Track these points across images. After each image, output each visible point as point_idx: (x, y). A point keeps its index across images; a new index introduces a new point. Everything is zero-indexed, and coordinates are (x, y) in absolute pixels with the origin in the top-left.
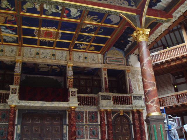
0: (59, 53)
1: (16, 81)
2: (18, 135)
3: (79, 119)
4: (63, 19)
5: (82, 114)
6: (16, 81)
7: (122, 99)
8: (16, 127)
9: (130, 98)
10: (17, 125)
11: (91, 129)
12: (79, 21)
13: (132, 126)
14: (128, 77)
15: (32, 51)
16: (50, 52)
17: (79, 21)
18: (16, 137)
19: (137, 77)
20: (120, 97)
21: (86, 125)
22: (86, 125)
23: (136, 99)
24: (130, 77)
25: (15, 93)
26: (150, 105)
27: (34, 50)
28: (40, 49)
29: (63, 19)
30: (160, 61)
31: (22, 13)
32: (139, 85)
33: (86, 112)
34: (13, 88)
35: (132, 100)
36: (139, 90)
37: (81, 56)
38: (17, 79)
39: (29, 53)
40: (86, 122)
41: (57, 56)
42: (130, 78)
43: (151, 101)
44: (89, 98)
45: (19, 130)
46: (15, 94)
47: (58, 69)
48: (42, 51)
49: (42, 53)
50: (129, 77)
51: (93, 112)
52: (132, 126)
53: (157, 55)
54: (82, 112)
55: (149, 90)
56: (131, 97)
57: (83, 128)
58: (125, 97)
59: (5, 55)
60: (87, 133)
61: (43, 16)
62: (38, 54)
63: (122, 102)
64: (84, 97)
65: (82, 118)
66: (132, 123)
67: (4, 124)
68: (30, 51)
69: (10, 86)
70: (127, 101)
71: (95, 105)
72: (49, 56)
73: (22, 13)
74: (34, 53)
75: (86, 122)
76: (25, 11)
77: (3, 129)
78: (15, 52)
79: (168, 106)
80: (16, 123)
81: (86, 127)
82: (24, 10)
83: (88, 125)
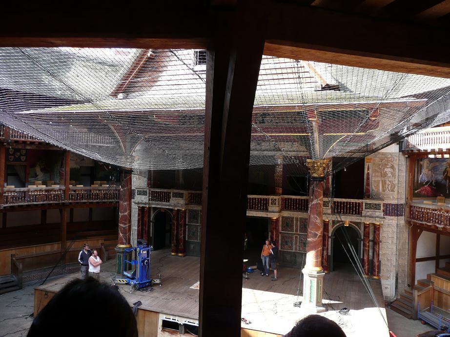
3: (287, 226)
5: (292, 221)
7: (347, 205)
11: (302, 240)
13: (362, 242)
14: (367, 169)
19: (384, 169)
20: (344, 202)
21: (296, 234)
22: (296, 234)
23: (370, 208)
24: (370, 170)
32: (385, 183)
33: (297, 219)
40: (297, 231)
42: (370, 171)
44: (303, 201)
50: (368, 169)
51: (304, 219)
52: (362, 242)
54: (292, 218)
57: (292, 238)
58: (353, 203)
60: (297, 243)
63: (347, 210)
64: (296, 199)
65: (292, 226)
66: (362, 238)
70: (356, 208)
75: (297, 231)
81: (296, 237)
83: (298, 234)
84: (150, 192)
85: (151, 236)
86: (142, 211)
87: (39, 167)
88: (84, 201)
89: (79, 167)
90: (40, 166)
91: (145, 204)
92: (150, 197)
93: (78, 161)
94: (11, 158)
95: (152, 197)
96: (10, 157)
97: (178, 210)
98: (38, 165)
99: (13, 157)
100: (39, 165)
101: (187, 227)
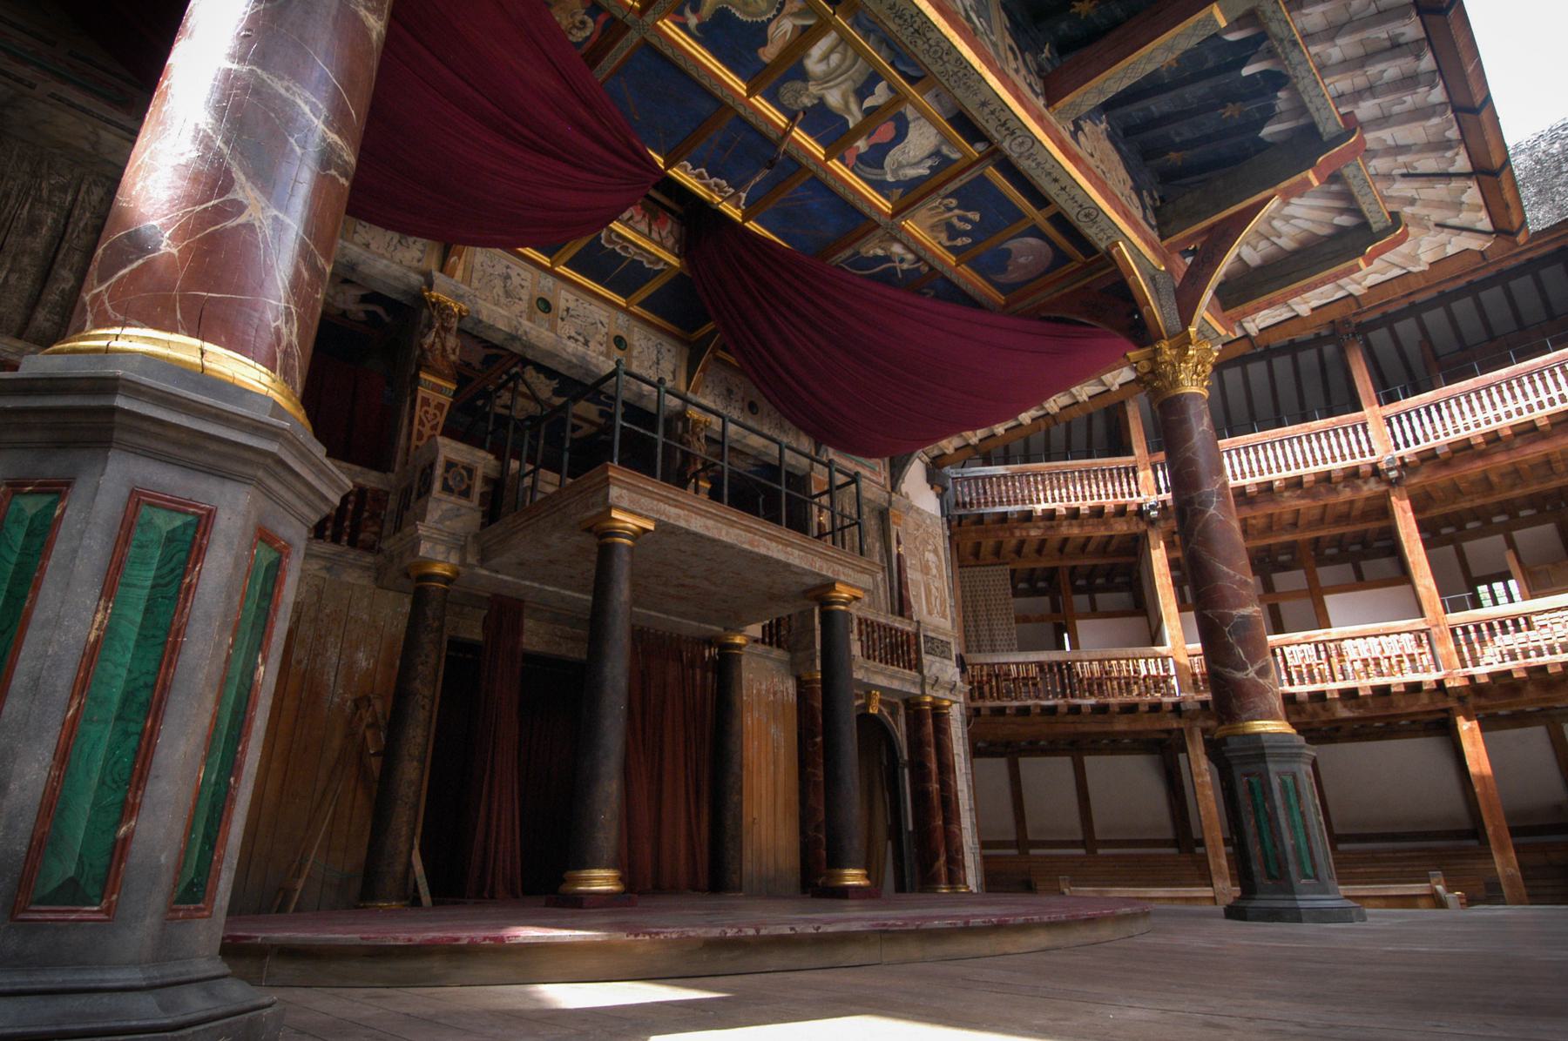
0: (643, 343)
1: (428, 426)
4: (835, 165)
6: (428, 426)
9: (913, 642)
12: (885, 206)
15: (516, 280)
16: (605, 321)
17: (885, 206)
25: (466, 494)
26: (1257, 685)
27: (524, 274)
28: (560, 284)
29: (835, 165)
30: (1018, 508)
31: (668, 27)
34: (453, 456)
35: (918, 651)
36: (930, 613)
37: (735, 390)
38: (431, 410)
39: (498, 283)
41: (635, 353)
43: (1256, 667)
46: (463, 502)
47: (586, 426)
48: (564, 299)
49: (568, 310)
50: (899, 543)
53: (1005, 476)
55: (1243, 617)
56: (917, 636)
58: (897, 630)
61: (759, 102)
62: (545, 305)
68: (508, 277)
71: (779, 646)
72: (599, 337)
73: (668, 27)
74: (525, 295)
76: (693, 21)
79: (1036, 706)
82: (695, 10)
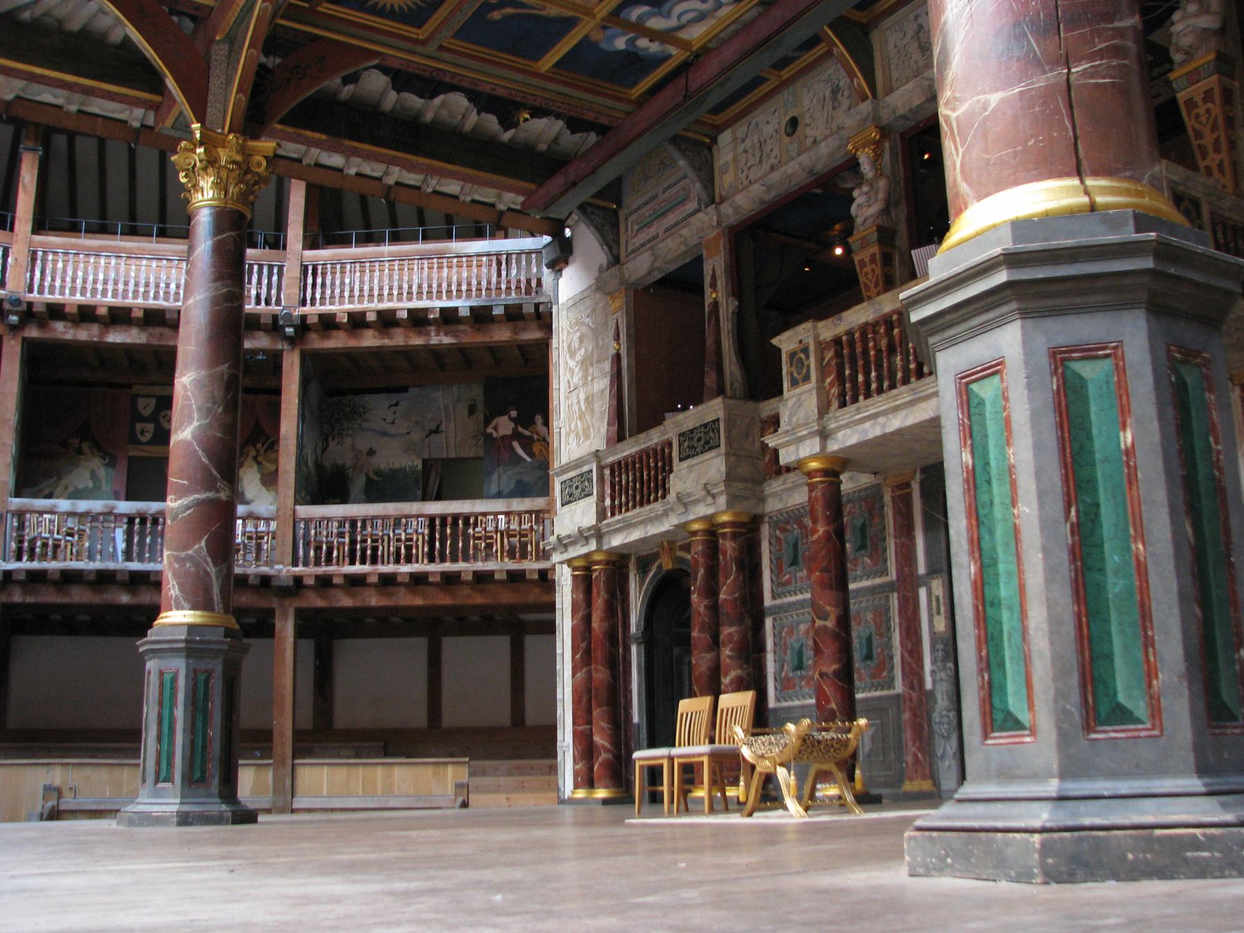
2: (940, 646)
6: (872, 285)
8: (923, 592)
10: (925, 581)
18: (934, 662)
45: (939, 613)
59: (809, 141)
67: (868, 588)
69: (775, 341)
77: (869, 616)
78: (846, 93)
80: (922, 570)
84: (607, 472)
85: (636, 719)
86: (584, 581)
87: (255, 467)
88: (358, 568)
89: (419, 464)
90: (259, 463)
91: (583, 536)
92: (608, 502)
93: (416, 436)
94: (142, 432)
95: (613, 500)
96: (139, 426)
97: (712, 531)
98: (250, 461)
99: (151, 427)
100: (255, 458)
101: (769, 622)
